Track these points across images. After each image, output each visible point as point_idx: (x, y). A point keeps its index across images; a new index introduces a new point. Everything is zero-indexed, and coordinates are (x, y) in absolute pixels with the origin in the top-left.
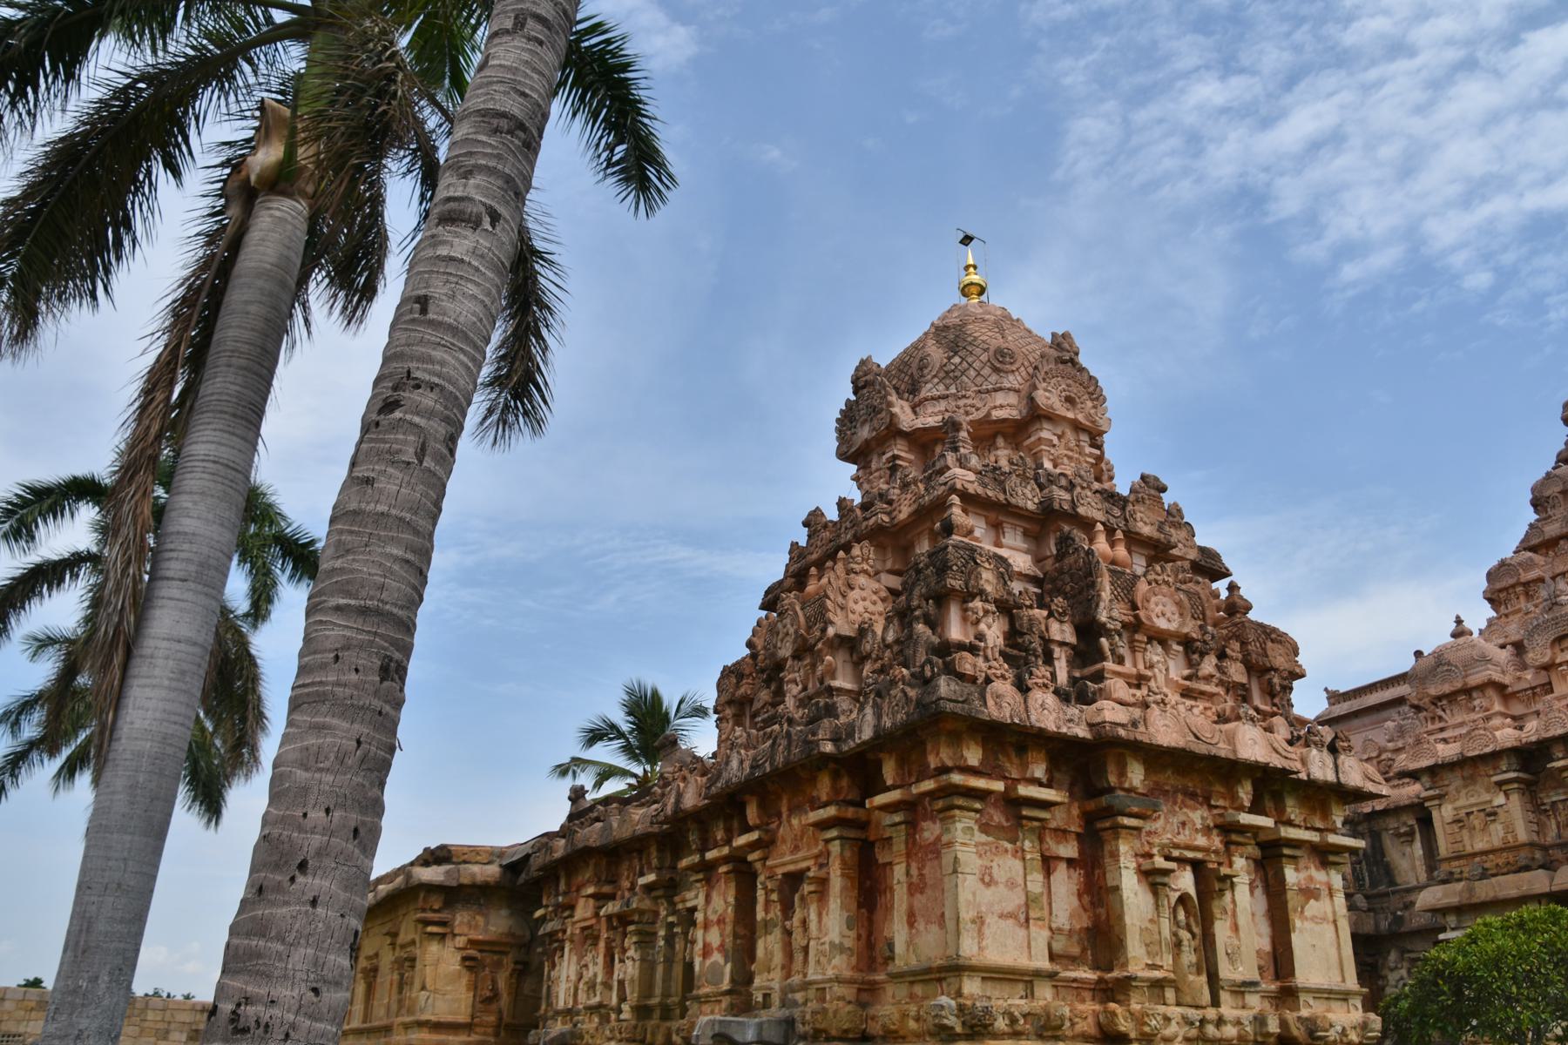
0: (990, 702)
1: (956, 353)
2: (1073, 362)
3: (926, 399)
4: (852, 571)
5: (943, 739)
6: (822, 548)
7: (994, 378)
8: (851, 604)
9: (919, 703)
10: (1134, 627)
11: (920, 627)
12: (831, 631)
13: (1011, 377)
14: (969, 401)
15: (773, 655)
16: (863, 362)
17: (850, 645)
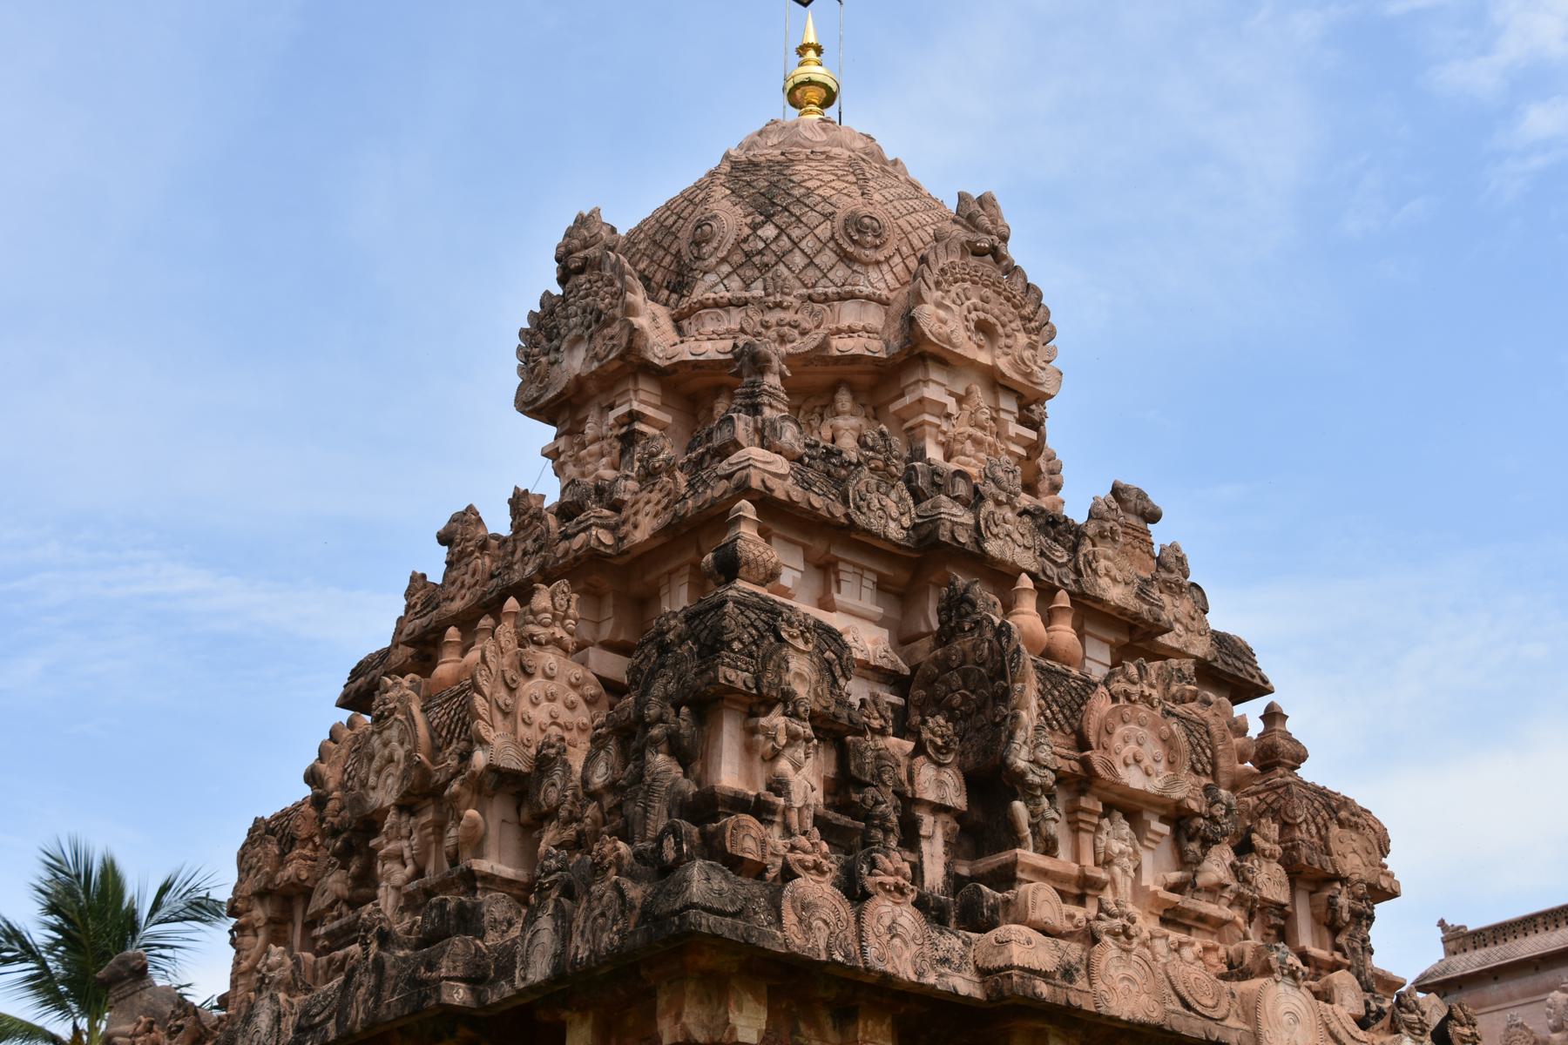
0: (789, 918)
1: (769, 218)
2: (996, 254)
3: (703, 305)
4: (531, 639)
5: (691, 986)
6: (476, 588)
7: (840, 273)
8: (524, 707)
9: (647, 913)
10: (1080, 781)
11: (660, 761)
12: (480, 759)
13: (874, 275)
14: (788, 316)
15: (359, 801)
16: (582, 221)
17: (516, 788)
